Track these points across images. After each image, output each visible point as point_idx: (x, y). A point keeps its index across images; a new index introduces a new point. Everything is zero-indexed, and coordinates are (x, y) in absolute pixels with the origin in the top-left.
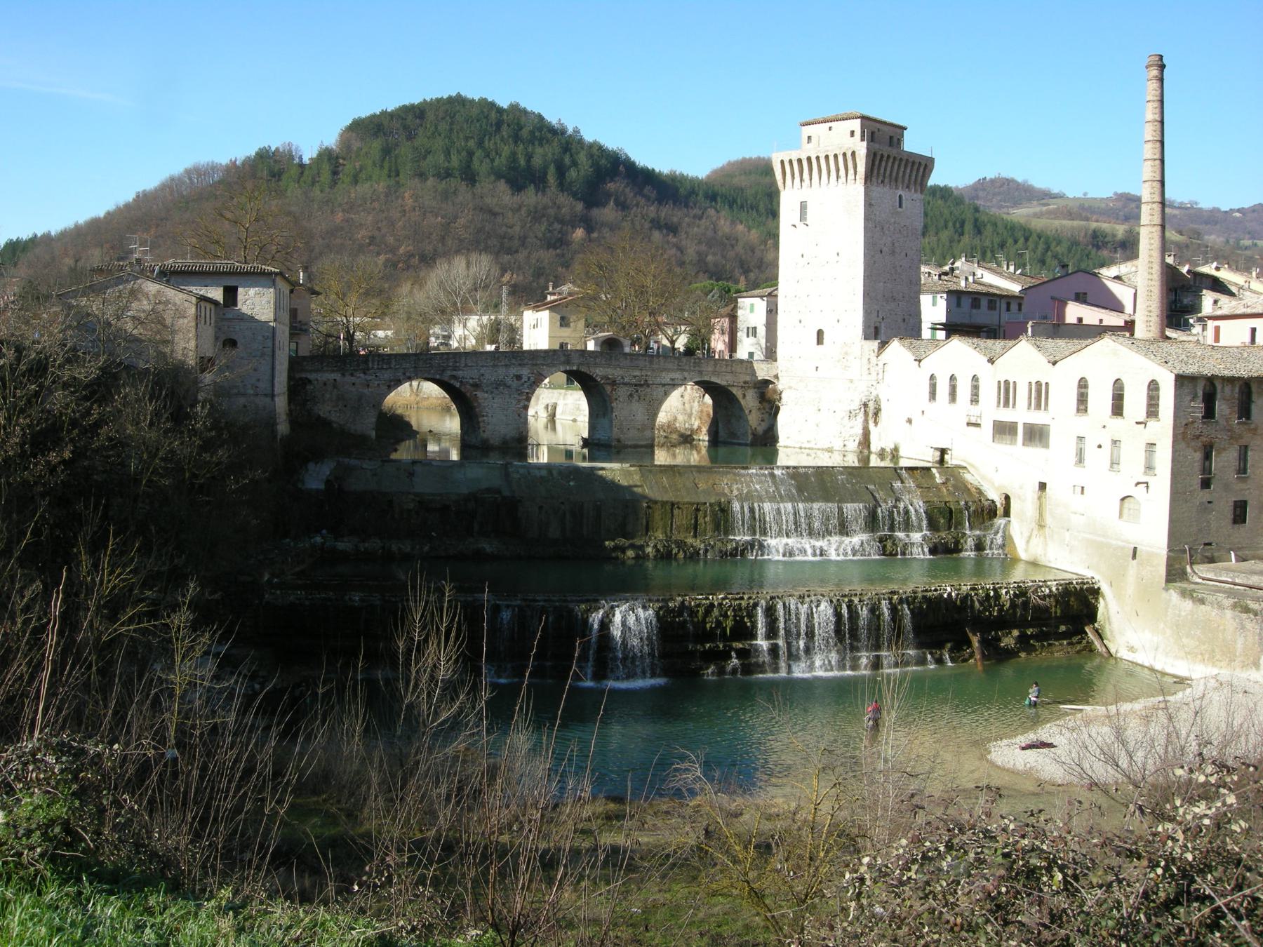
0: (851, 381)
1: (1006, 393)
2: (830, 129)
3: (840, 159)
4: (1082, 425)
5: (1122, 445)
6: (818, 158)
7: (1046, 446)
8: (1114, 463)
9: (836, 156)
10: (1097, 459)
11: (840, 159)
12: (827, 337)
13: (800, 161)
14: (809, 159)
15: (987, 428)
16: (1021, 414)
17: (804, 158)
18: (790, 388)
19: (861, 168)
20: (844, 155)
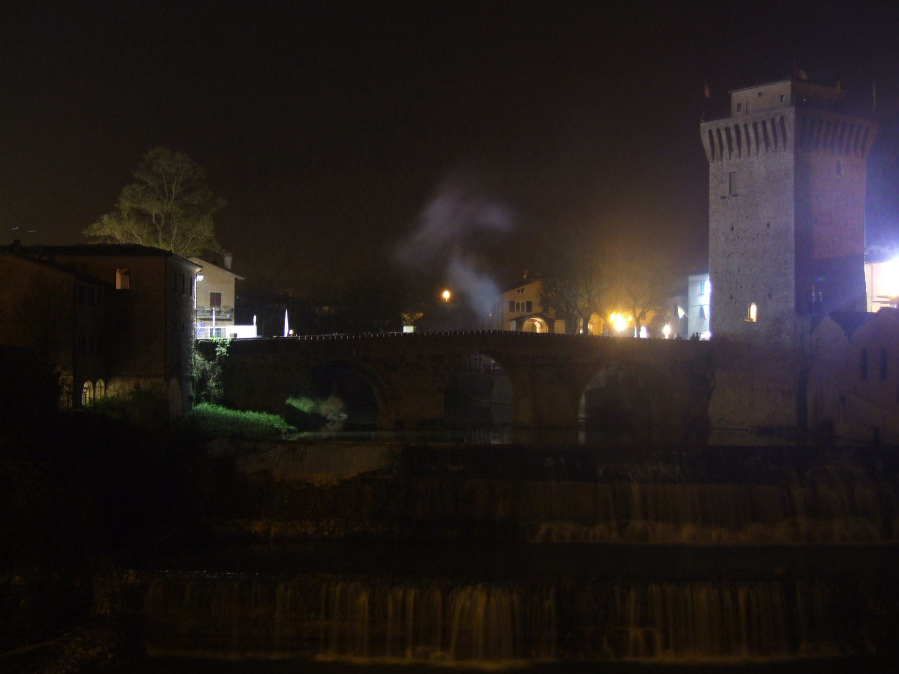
2: (760, 95)
3: (769, 126)
9: (764, 123)
11: (769, 126)
13: (727, 130)
14: (737, 127)
19: (790, 135)
20: (773, 121)
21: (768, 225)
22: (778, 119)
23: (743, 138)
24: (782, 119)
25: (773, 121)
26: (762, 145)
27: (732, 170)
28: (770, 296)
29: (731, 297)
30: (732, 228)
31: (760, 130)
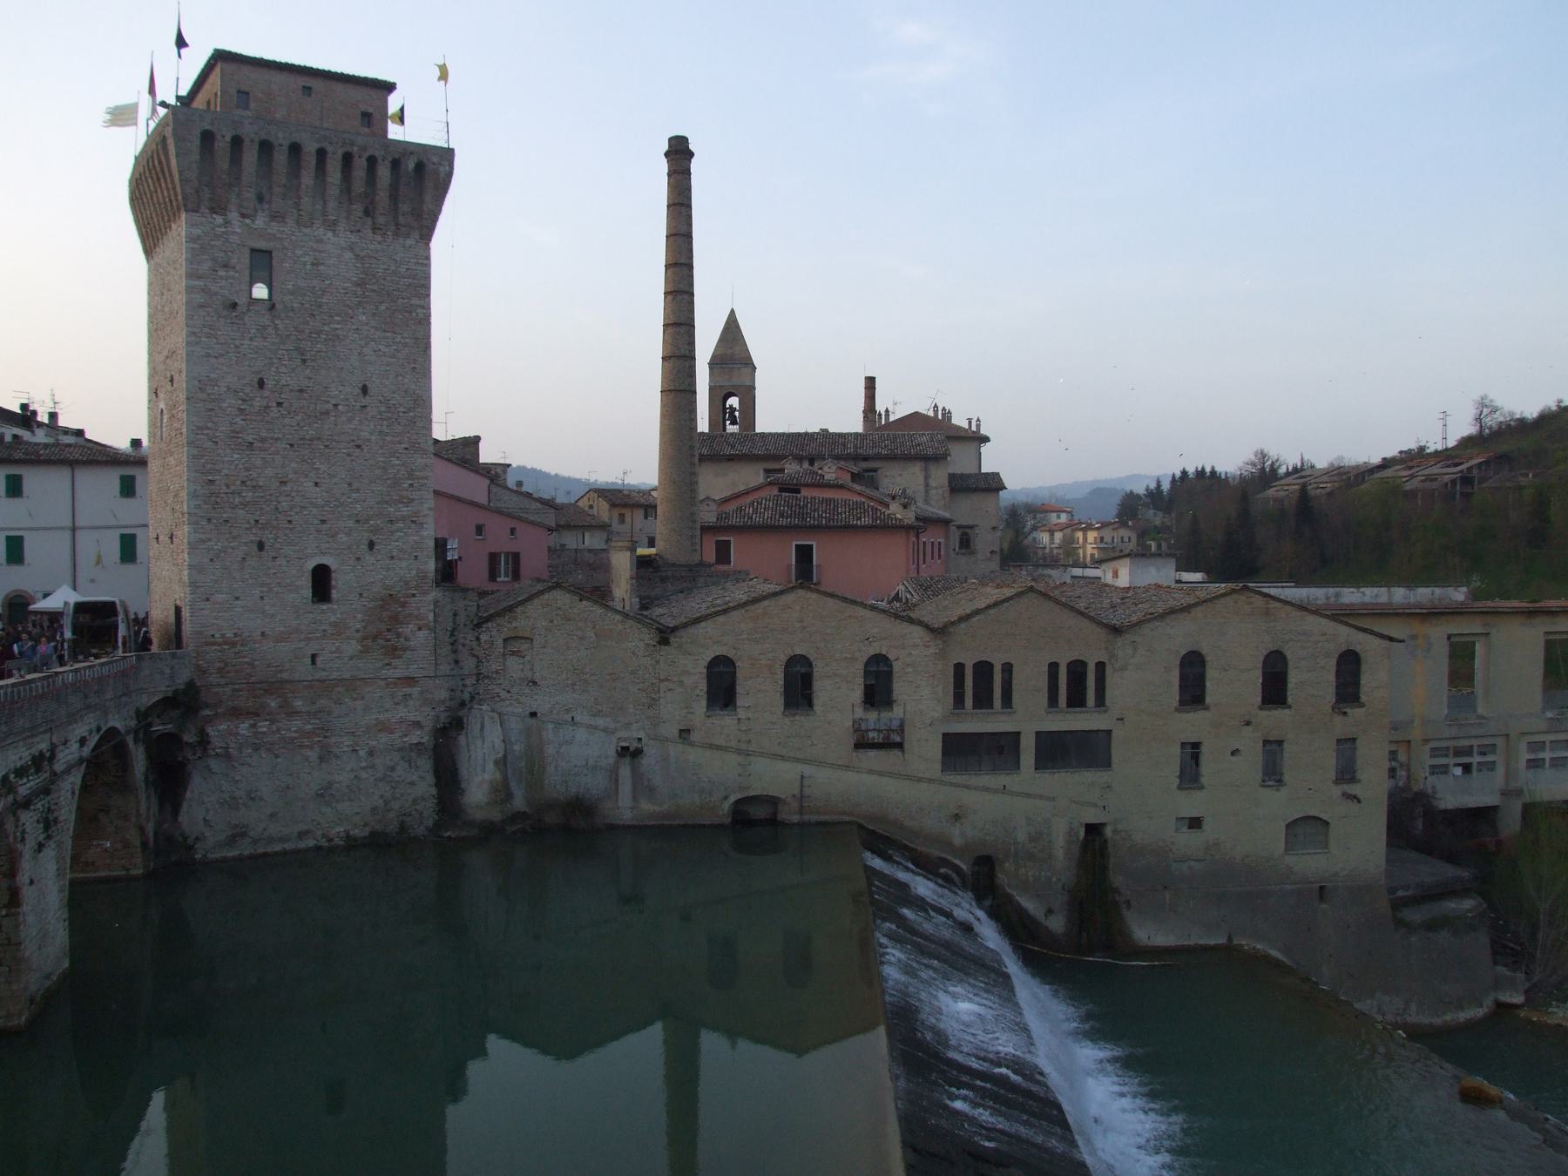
0: (410, 681)
1: (981, 684)
2: (307, 90)
3: (384, 172)
4: (1192, 724)
5: (1286, 745)
6: (321, 154)
7: (1107, 764)
8: (1272, 773)
9: (372, 161)
10: (1232, 768)
11: (384, 172)
12: (341, 582)
14: (295, 149)
15: (926, 749)
16: (1030, 716)
17: (281, 139)
18: (236, 713)
21: (365, 390)
22: (411, 166)
23: (307, 179)
24: (420, 167)
25: (396, 164)
26: (358, 208)
27: (262, 244)
28: (371, 545)
29: (261, 546)
30: (261, 384)
31: (359, 172)
